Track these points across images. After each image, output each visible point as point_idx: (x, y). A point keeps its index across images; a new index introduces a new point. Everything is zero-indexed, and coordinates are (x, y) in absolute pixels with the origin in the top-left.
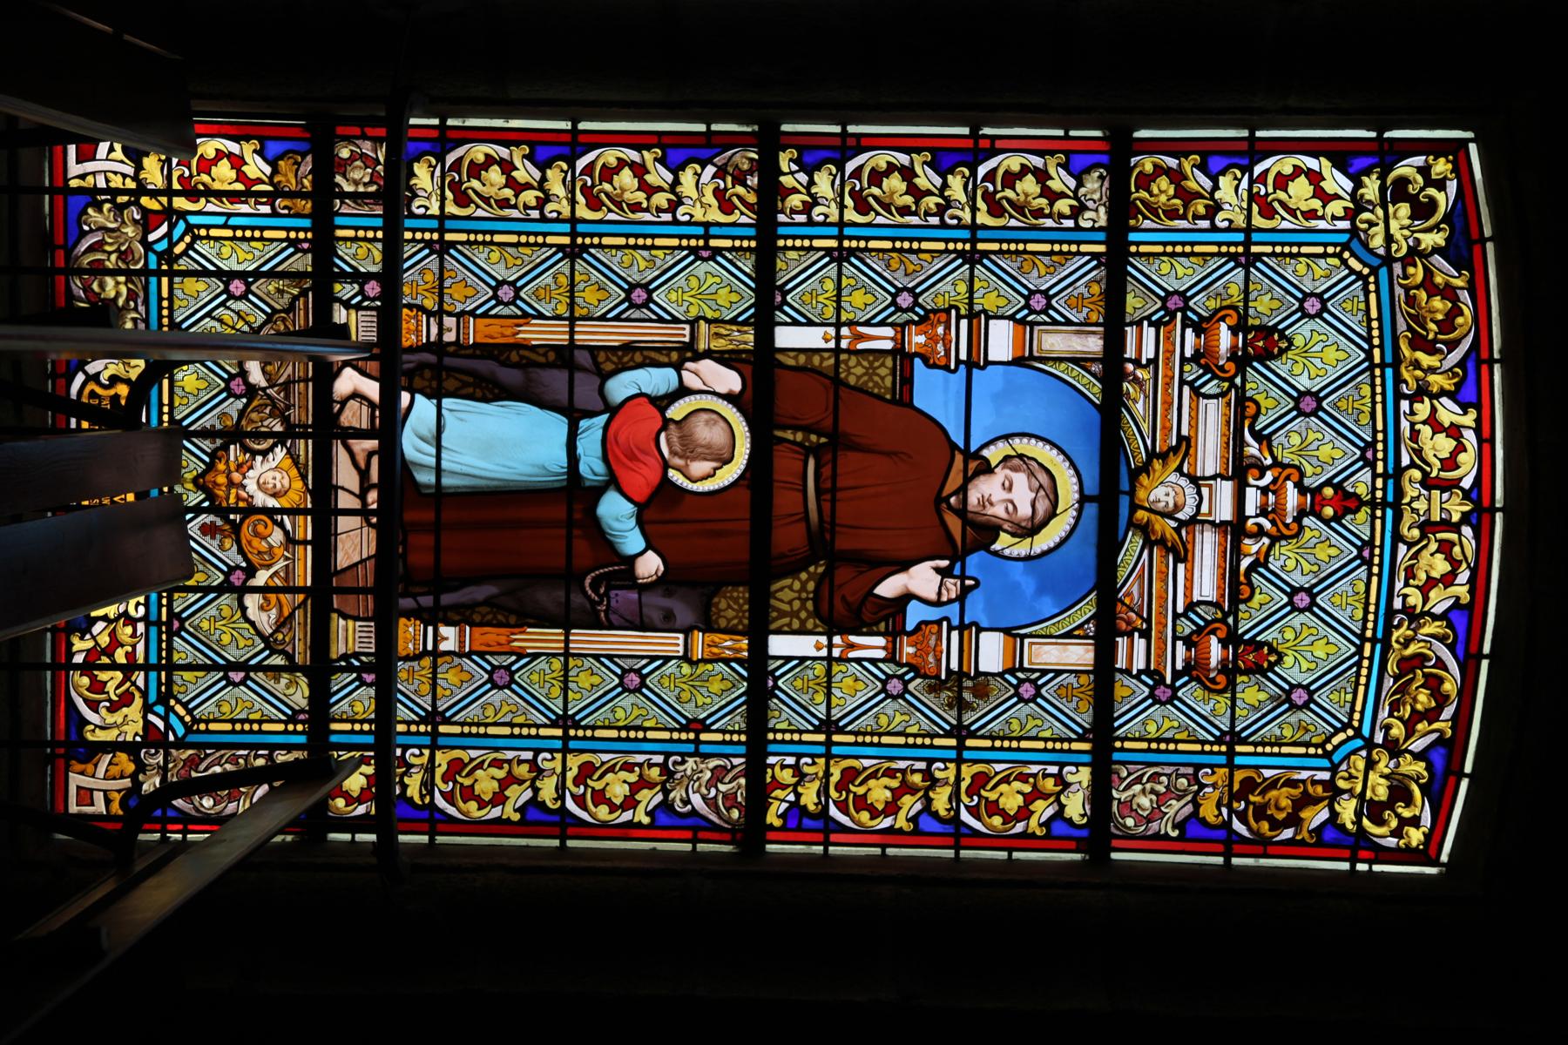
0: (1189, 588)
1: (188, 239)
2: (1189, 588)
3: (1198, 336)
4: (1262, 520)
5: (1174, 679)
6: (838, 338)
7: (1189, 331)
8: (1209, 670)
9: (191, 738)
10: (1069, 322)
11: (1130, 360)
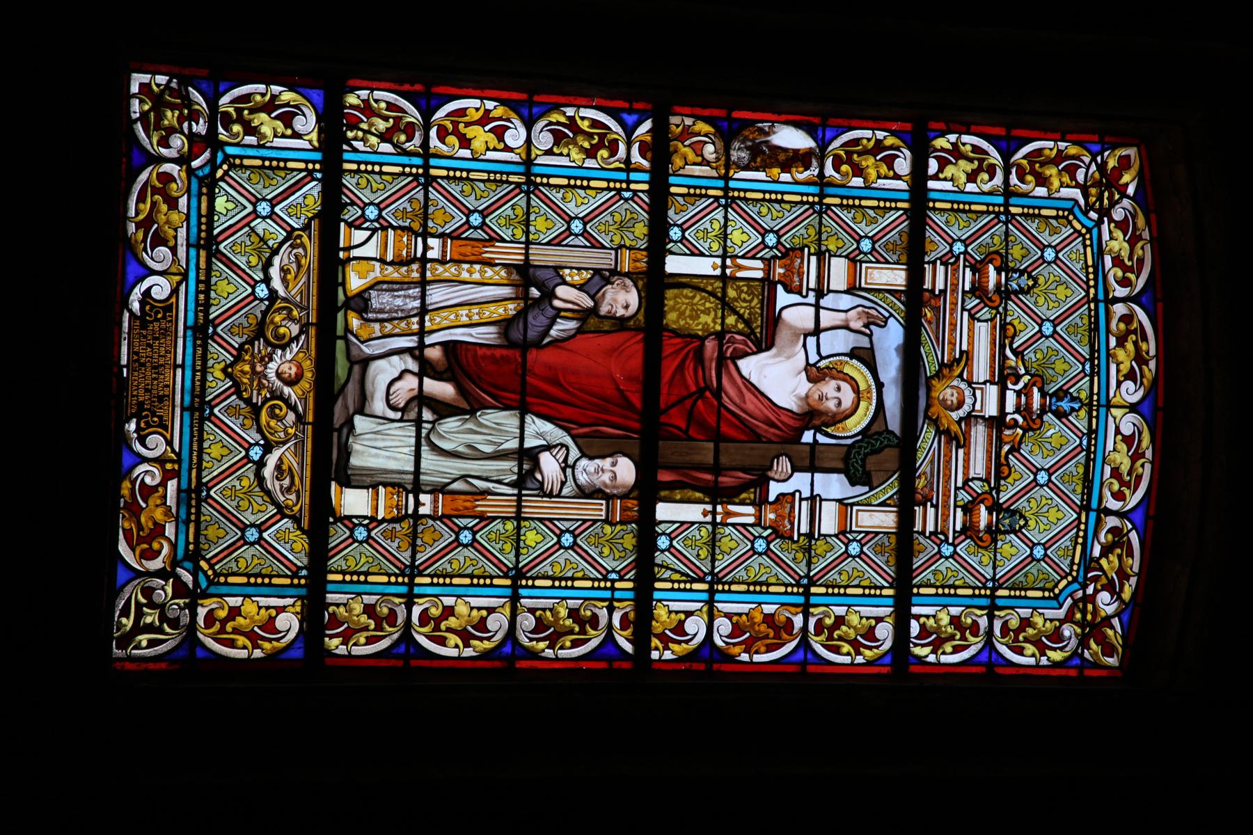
0: (966, 468)
1: (225, 167)
2: (966, 468)
3: (974, 274)
4: (1017, 416)
5: (954, 538)
6: (724, 267)
7: (968, 270)
8: (979, 531)
9: (212, 590)
10: (887, 262)
11: (927, 290)
